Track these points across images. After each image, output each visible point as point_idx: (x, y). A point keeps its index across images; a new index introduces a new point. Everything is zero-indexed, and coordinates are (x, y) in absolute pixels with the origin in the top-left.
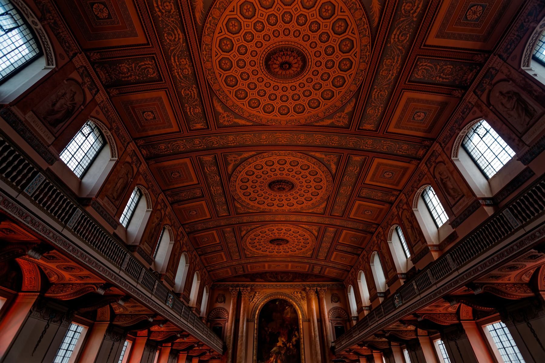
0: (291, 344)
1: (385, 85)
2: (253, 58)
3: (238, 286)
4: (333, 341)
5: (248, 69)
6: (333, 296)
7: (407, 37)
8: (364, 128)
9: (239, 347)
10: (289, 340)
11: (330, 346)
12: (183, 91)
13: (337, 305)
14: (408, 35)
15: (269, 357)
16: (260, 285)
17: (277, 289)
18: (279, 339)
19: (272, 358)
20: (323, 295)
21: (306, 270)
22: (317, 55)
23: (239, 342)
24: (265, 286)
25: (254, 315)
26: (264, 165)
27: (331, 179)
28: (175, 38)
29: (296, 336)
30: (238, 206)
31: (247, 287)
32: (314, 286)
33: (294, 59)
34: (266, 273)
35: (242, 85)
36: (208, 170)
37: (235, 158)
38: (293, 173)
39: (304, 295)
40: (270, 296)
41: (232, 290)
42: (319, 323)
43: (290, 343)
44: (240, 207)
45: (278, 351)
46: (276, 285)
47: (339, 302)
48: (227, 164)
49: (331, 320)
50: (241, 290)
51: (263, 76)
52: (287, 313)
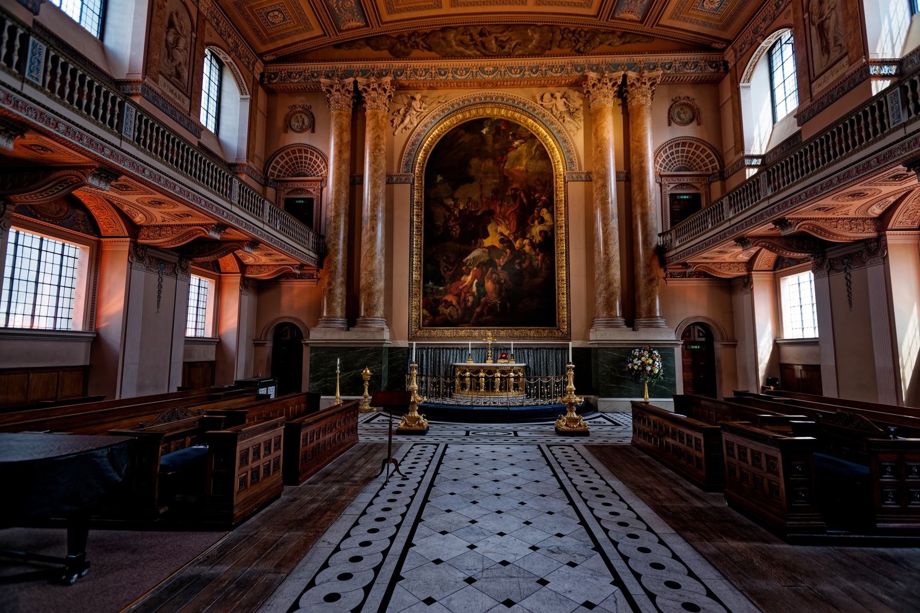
0: (526, 241)
3: (348, 73)
4: (660, 231)
6: (675, 103)
9: (365, 248)
10: (522, 229)
11: (654, 245)
13: (688, 131)
15: (458, 275)
16: (427, 71)
17: (482, 85)
18: (490, 228)
19: (469, 278)
20: (642, 98)
21: (592, 11)
23: (364, 232)
24: (440, 72)
25: (410, 166)
29: (542, 221)
31: (380, 75)
32: (616, 67)
34: (443, 30)
39: (577, 101)
40: (461, 109)
41: (332, 87)
42: (623, 183)
43: (524, 238)
45: (485, 258)
46: (481, 69)
47: (694, 123)
49: (661, 176)
50: (360, 87)
52: (518, 159)
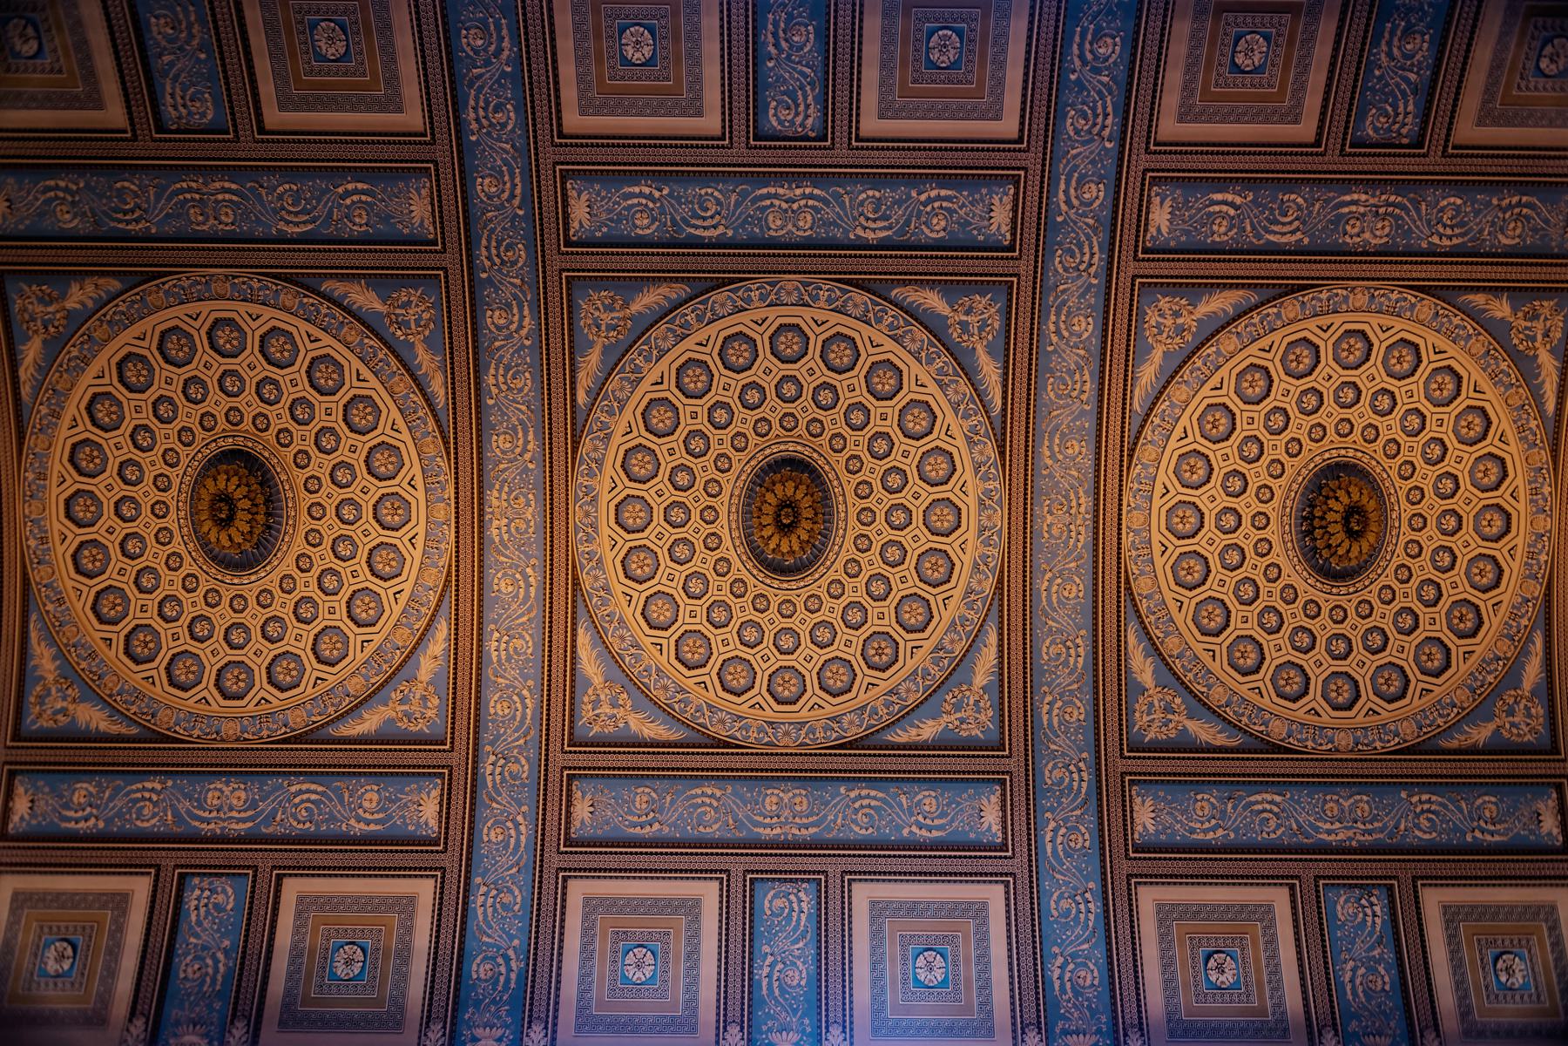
1: (842, 205)
2: (774, 607)
5: (803, 622)
7: (707, 194)
8: (1004, 229)
12: (857, 829)
14: (703, 192)
22: (763, 428)
26: (1202, 593)
27: (1290, 307)
28: (710, 805)
30: (1481, 734)
33: (773, 491)
35: (849, 645)
36: (1214, 829)
37: (1151, 705)
38: (1257, 474)
44: (1491, 727)
48: (1185, 746)
51: (824, 582)
